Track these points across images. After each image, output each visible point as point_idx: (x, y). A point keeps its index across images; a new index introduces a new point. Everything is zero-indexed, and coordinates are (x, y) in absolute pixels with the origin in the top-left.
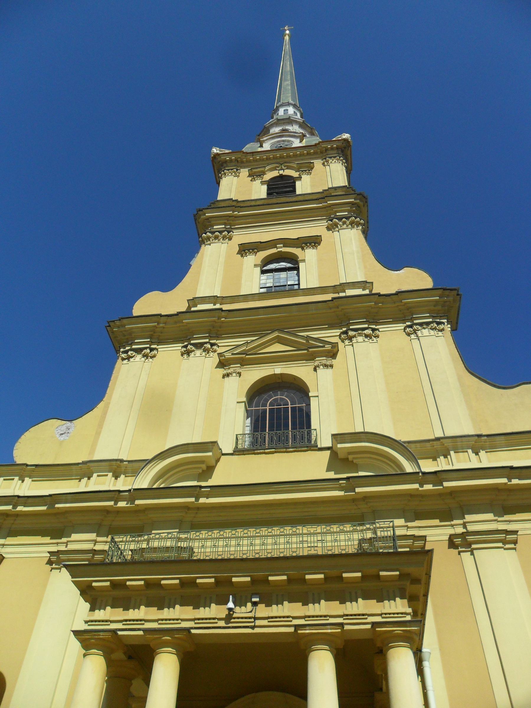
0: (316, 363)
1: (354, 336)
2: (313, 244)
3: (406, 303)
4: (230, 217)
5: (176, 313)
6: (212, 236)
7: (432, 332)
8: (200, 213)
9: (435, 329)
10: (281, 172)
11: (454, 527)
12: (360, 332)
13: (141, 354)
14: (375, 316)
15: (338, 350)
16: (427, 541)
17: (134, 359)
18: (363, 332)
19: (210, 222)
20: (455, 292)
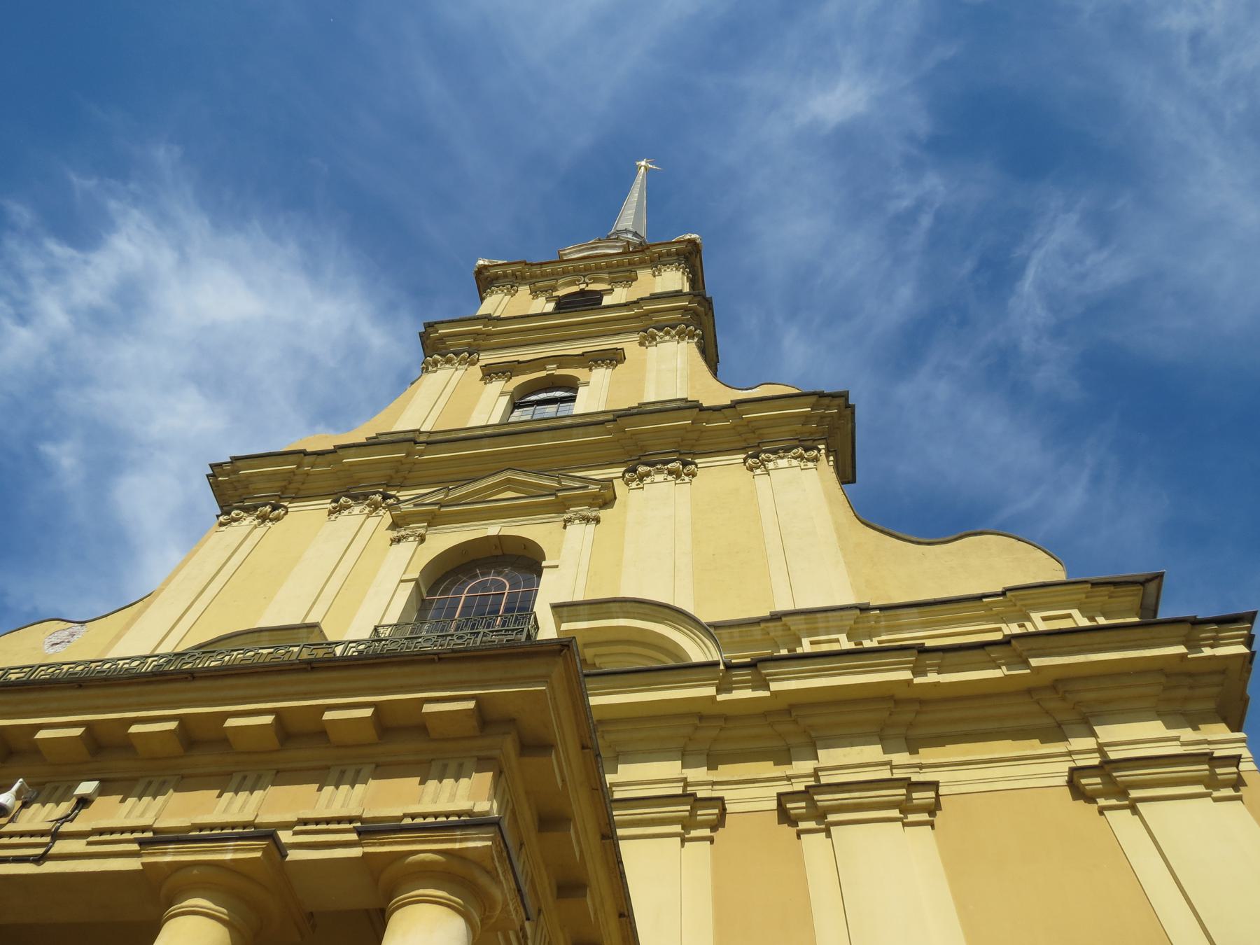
0: (566, 516)
1: (648, 474)
2: (608, 361)
3: (750, 421)
4: (478, 335)
5: (333, 448)
6: (441, 360)
7: (795, 462)
8: (430, 330)
9: (801, 457)
10: (583, 286)
11: (793, 780)
12: (659, 467)
13: (251, 515)
14: (693, 446)
15: (615, 498)
16: (727, 812)
17: (240, 523)
18: (666, 467)
19: (445, 343)
20: (841, 401)
